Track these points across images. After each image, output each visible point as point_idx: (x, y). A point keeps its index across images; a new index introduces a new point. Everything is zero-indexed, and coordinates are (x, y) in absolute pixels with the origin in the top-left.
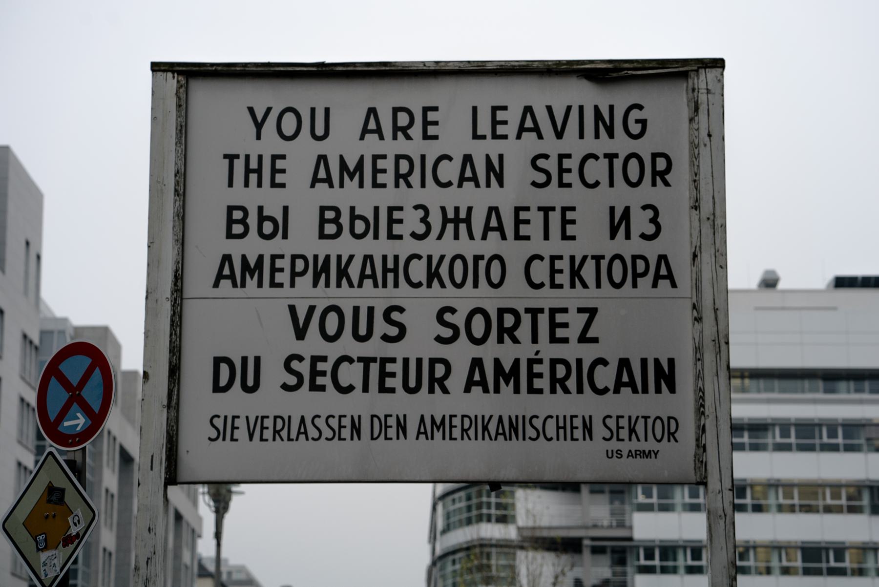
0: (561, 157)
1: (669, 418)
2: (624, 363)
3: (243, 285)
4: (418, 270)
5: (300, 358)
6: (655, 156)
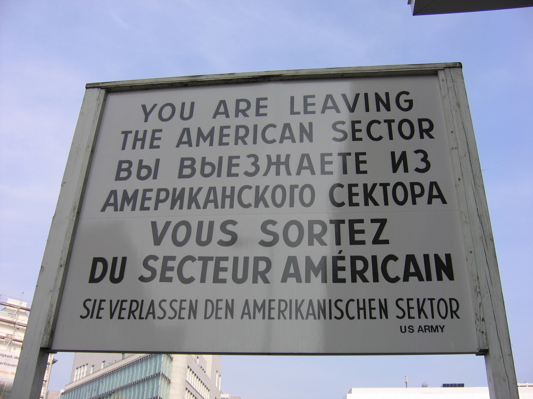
0: (353, 123)
1: (451, 300)
2: (410, 259)
3: (122, 209)
4: (249, 197)
5: (155, 258)
6: (420, 121)
